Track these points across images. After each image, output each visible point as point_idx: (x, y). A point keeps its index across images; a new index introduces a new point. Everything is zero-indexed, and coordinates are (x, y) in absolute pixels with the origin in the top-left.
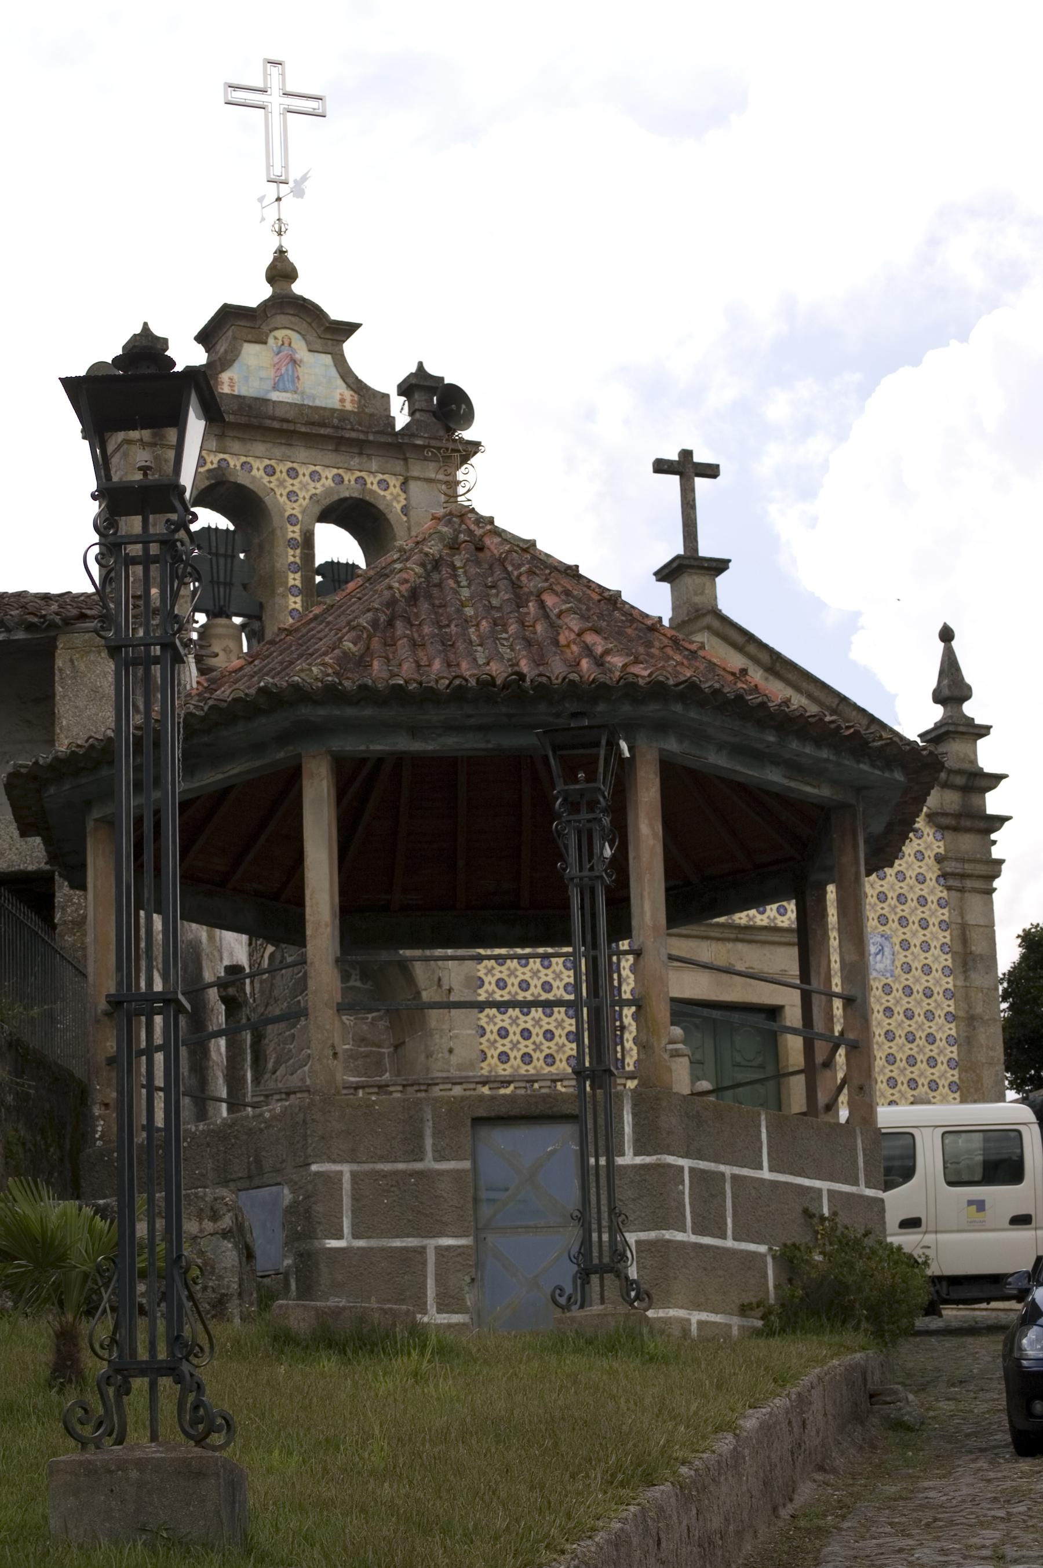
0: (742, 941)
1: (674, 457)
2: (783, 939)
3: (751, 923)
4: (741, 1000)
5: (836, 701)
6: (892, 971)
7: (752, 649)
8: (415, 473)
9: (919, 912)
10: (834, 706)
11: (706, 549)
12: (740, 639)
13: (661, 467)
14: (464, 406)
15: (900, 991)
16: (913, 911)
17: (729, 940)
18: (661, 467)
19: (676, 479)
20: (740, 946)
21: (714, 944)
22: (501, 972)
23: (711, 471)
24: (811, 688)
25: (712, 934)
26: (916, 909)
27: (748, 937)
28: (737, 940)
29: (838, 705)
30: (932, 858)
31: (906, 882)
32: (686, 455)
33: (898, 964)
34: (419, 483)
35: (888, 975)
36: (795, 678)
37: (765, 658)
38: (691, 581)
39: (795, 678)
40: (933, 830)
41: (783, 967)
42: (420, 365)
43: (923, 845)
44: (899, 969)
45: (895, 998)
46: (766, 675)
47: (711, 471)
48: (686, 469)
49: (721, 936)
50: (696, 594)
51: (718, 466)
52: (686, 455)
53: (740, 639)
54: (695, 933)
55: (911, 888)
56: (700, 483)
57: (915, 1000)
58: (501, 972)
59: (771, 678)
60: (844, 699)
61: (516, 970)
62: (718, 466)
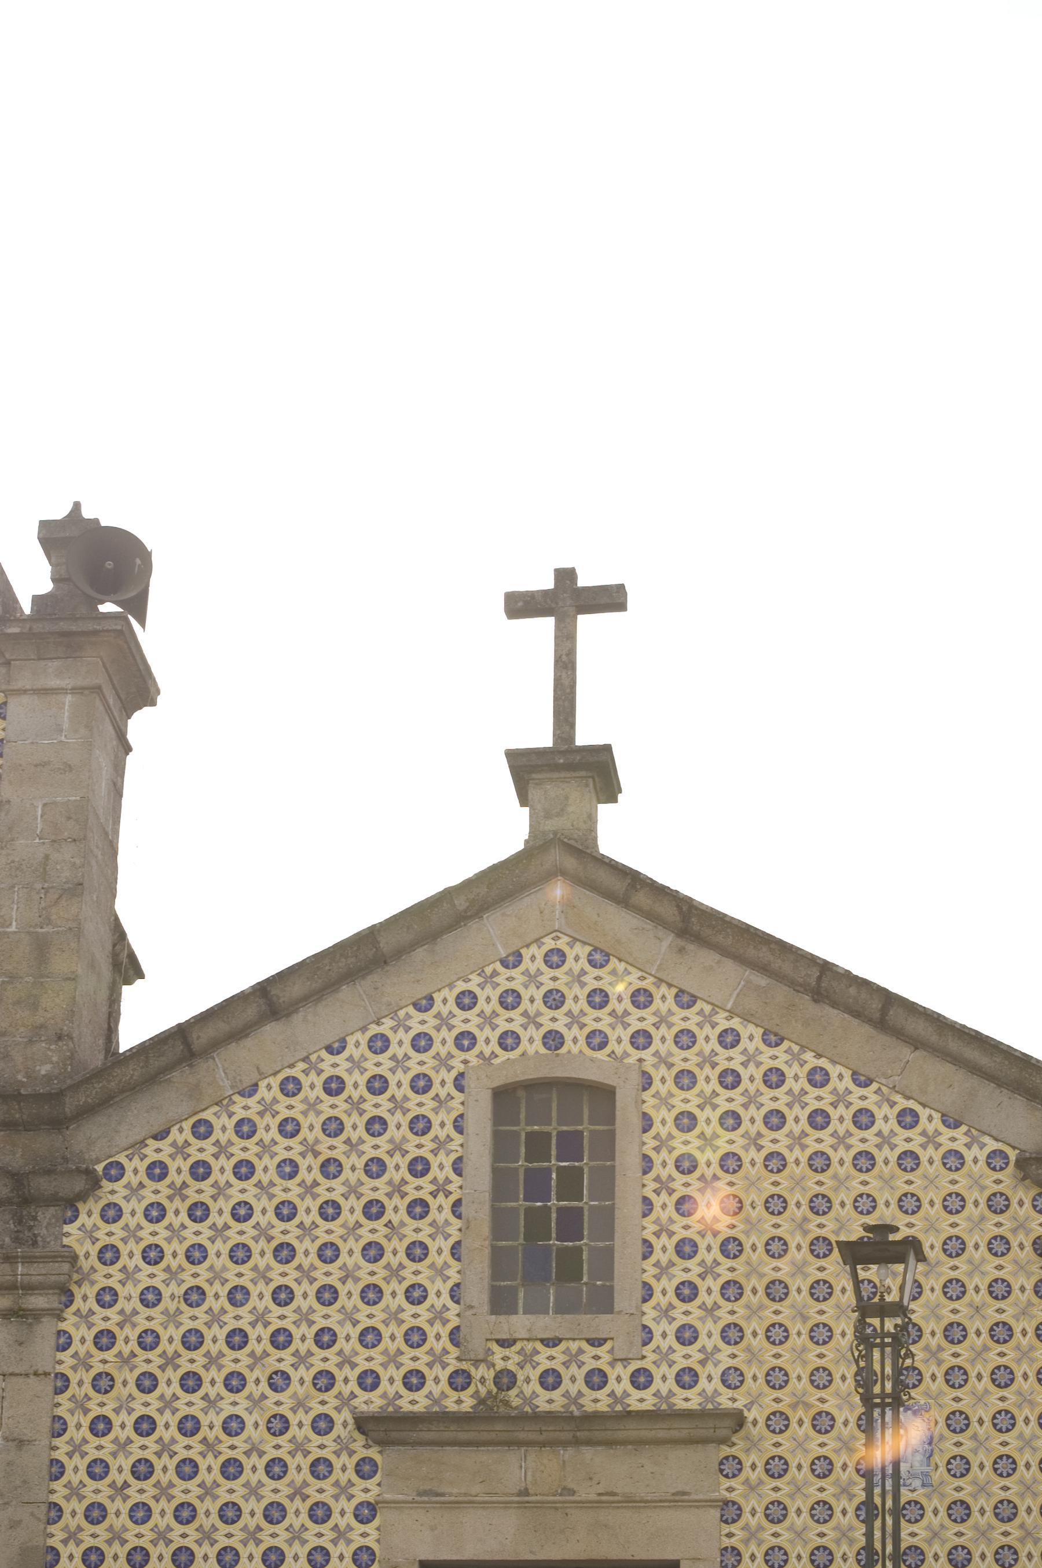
0: (589, 1443)
1: (549, 584)
2: (675, 1434)
3: (710, 1406)
4: (583, 1556)
5: (815, 973)
6: (926, 1475)
7: (641, 898)
8: (24, 681)
9: (992, 1355)
10: (813, 982)
11: (584, 736)
12: (619, 886)
13: (521, 605)
14: (138, 561)
15: (943, 1512)
16: (980, 1354)
17: (565, 1444)
18: (521, 605)
19: (546, 625)
20: (588, 1453)
21: (533, 1454)
22: (94, 1536)
23: (610, 599)
24: (764, 954)
25: (522, 1436)
26: (986, 1348)
27: (599, 1435)
28: (577, 1442)
29: (819, 978)
30: (1028, 1248)
31: (966, 1299)
32: (565, 576)
33: (940, 1459)
34: (25, 699)
35: (917, 1483)
36: (729, 941)
37: (668, 912)
38: (549, 790)
39: (729, 941)
40: (1033, 1192)
41: (680, 1488)
42: (77, 506)
43: (1008, 1225)
44: (942, 1469)
45: (928, 1528)
46: (681, 942)
47: (610, 599)
48: (567, 601)
49: (541, 1438)
50: (548, 816)
51: (621, 587)
52: (565, 576)
53: (619, 886)
54: (485, 1436)
55: (977, 1309)
56: (587, 624)
57: (976, 1527)
58: (94, 1536)
59: (691, 947)
60: (826, 967)
61: (66, 1529)
62: (621, 587)
